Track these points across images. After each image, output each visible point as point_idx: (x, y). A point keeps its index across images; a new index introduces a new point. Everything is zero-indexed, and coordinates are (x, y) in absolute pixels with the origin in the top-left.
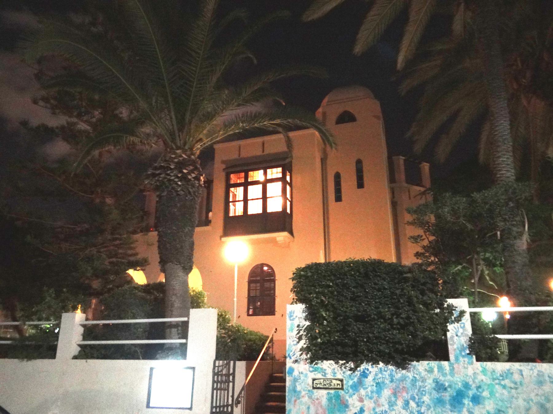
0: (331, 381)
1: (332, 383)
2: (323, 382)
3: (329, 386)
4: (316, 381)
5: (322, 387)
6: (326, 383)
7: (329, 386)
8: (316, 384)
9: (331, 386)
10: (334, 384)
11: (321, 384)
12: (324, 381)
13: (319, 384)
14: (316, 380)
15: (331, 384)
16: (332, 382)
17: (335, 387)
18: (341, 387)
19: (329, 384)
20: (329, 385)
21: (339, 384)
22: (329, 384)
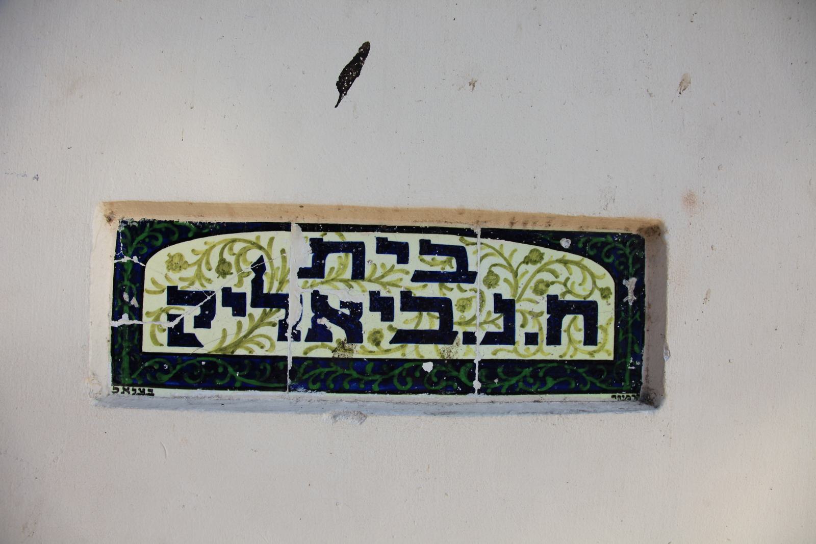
0: (459, 254)
1: (454, 292)
2: (316, 271)
3: (402, 337)
4: (185, 249)
5: (292, 350)
6: (360, 294)
7: (402, 337)
8: (176, 296)
9: (445, 335)
10: (505, 307)
11: (280, 301)
12: (320, 250)
13: (235, 301)
14: (203, 230)
15: (443, 307)
16: (464, 275)
17: (519, 351)
18: (605, 350)
19: (410, 302)
20: (405, 320)
21: (588, 310)
22: (410, 302)
